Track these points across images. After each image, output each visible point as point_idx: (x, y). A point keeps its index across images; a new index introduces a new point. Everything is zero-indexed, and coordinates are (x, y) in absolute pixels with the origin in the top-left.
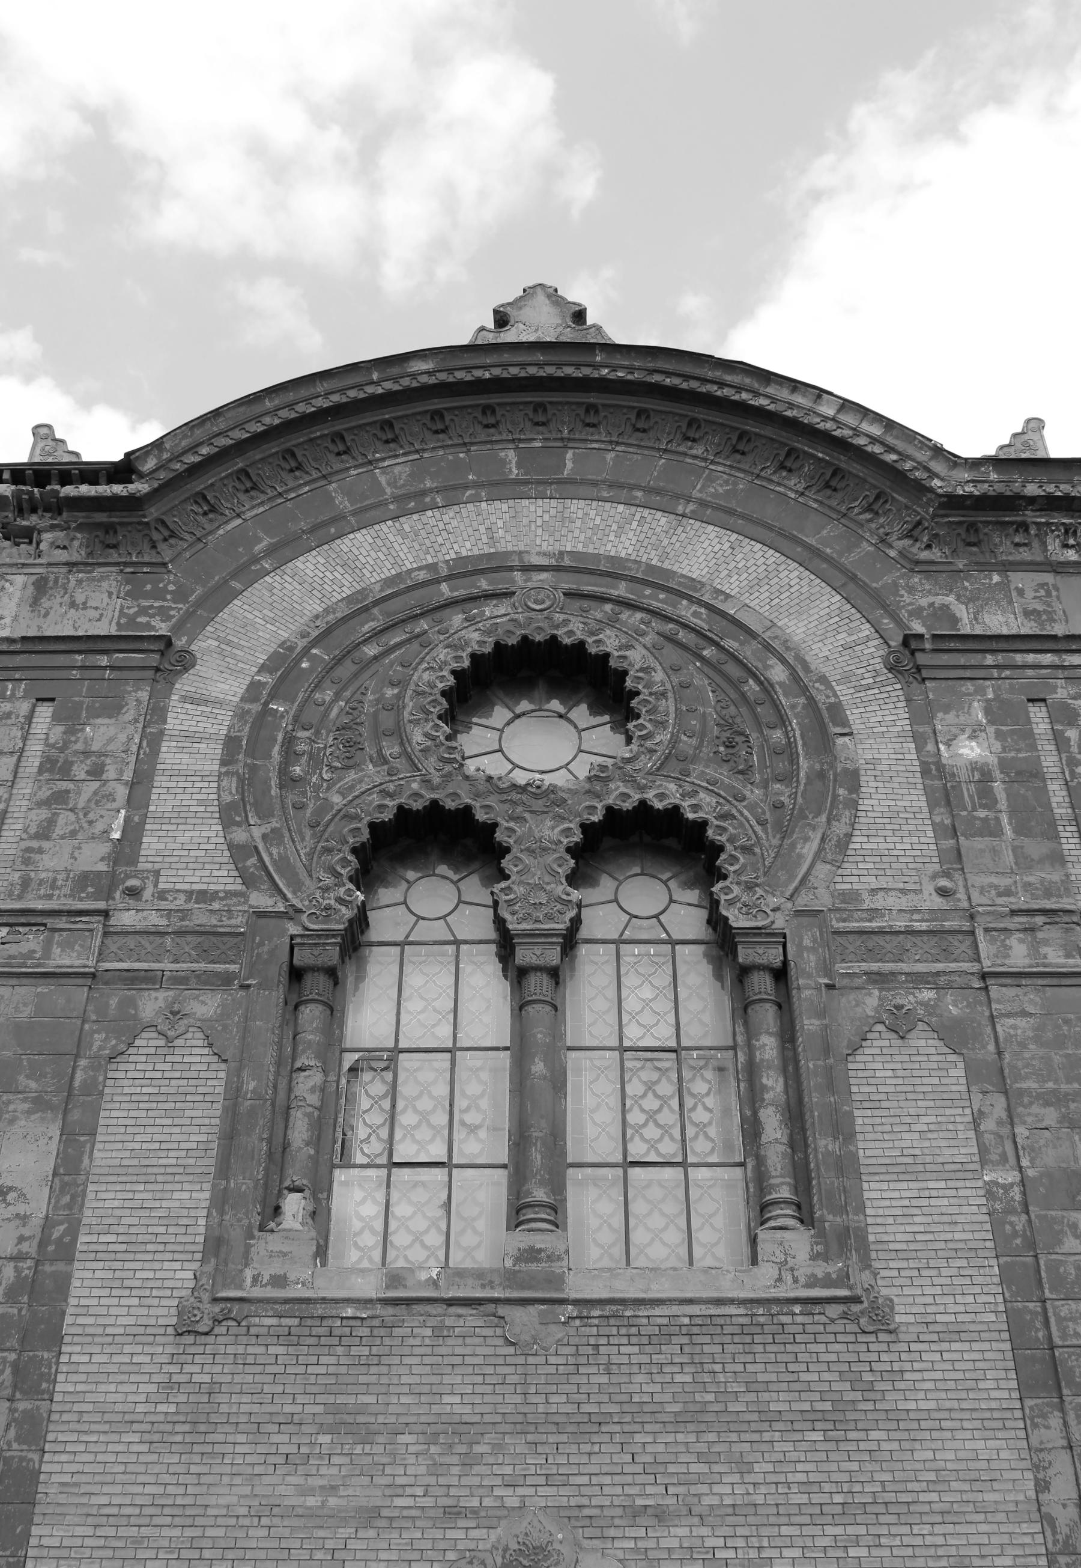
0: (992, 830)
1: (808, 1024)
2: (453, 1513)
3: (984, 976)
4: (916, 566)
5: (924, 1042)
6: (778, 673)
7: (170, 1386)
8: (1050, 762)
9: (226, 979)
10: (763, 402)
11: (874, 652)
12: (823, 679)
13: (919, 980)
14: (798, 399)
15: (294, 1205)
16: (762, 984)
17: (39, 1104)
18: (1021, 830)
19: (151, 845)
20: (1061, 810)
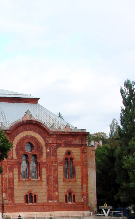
0: (49, 156)
1: (40, 167)
2: (28, 189)
3: (47, 165)
4: (47, 137)
5: (45, 168)
6: (40, 145)
7: (18, 184)
8: (52, 151)
9: (17, 165)
10: (41, 125)
11: (44, 143)
12: (42, 146)
13: (45, 165)
14: (44, 126)
15: (21, 176)
16: (38, 165)
17: (11, 171)
18: (50, 156)
19: (13, 156)
20: (52, 155)
